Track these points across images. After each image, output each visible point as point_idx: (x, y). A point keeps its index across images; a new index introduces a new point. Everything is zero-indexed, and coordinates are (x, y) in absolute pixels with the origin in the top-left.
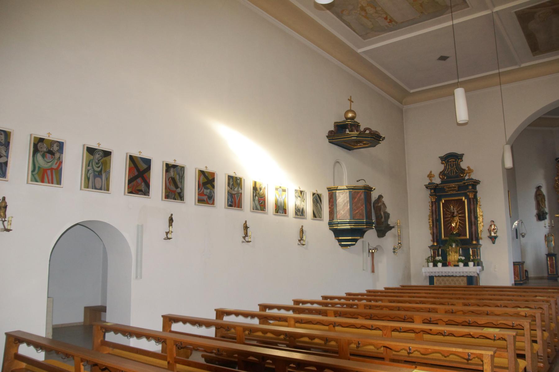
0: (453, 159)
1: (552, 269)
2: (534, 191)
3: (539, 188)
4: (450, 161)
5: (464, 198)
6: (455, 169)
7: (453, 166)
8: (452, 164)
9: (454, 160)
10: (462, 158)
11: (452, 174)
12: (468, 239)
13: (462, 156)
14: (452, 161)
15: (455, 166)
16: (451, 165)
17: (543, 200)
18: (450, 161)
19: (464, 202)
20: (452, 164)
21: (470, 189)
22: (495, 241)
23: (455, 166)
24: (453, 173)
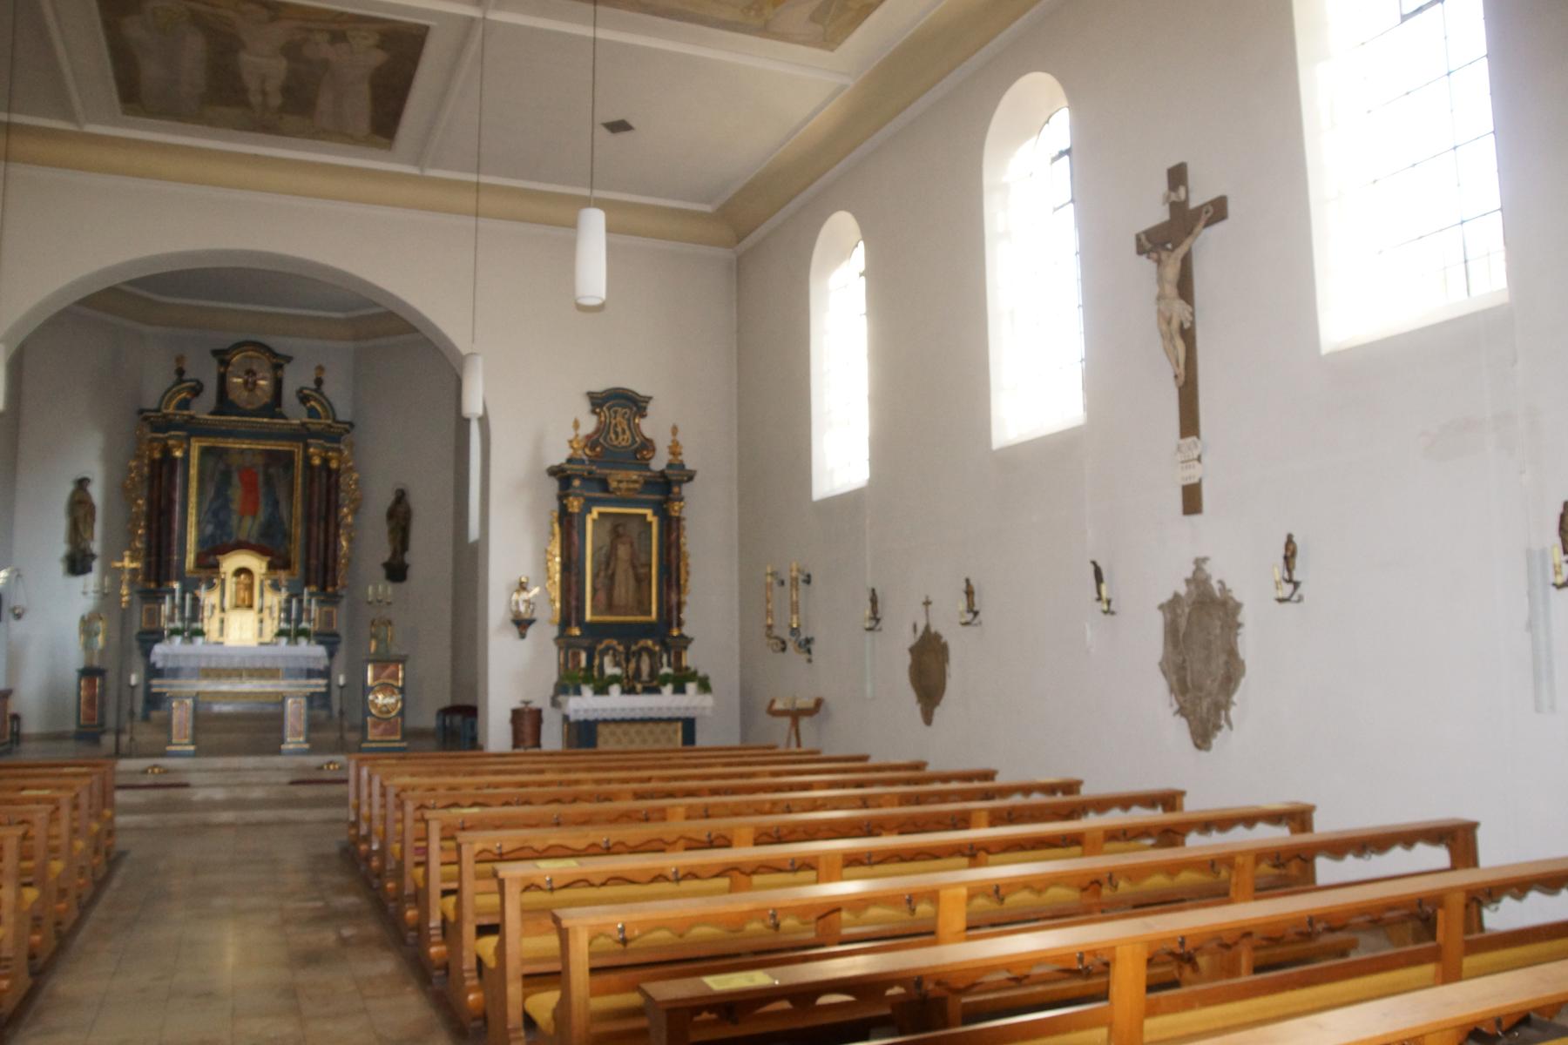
2: (68, 488)
3: (82, 484)
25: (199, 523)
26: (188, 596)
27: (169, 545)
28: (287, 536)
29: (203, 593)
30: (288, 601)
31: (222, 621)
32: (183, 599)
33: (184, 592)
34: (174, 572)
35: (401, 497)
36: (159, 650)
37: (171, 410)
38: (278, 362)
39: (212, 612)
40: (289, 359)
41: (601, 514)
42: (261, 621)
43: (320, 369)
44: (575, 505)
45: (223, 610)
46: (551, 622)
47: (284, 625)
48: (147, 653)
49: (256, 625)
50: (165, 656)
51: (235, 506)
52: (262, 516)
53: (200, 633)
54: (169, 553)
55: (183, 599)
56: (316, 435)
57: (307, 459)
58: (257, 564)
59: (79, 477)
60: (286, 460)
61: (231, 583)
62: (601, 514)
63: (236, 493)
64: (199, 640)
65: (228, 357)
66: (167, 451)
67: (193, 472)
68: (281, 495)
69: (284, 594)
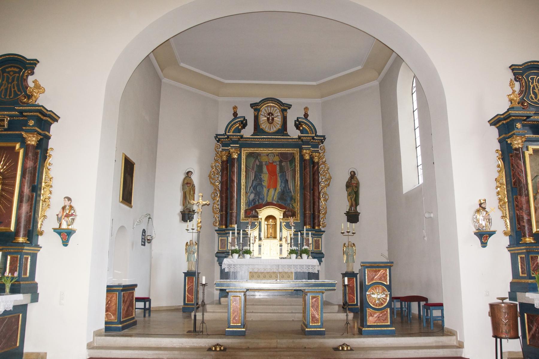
0: (14, 67)
1: (190, 296)
2: (183, 177)
3: (189, 173)
4: (9, 69)
5: (18, 146)
6: (14, 88)
7: (13, 81)
8: (11, 78)
9: (17, 70)
10: (34, 68)
11: (7, 97)
12: (12, 232)
13: (36, 64)
14: (13, 71)
15: (15, 82)
16: (8, 78)
17: (192, 192)
18: (7, 70)
19: (18, 153)
20: (11, 78)
21: (29, 126)
22: (68, 241)
23: (15, 82)
24: (10, 95)
25: (246, 193)
26: (241, 232)
27: (232, 204)
28: (292, 199)
29: (249, 231)
30: (296, 235)
31: (260, 246)
32: (239, 234)
33: (239, 230)
34: (234, 219)
35: (353, 175)
36: (226, 261)
37: (231, 134)
38: (285, 108)
39: (255, 241)
40: (289, 106)
41: (534, 150)
42: (281, 246)
43: (306, 109)
44: (517, 143)
45: (260, 239)
46: (505, 234)
47: (294, 248)
48: (220, 264)
49: (279, 248)
50: (229, 265)
51: (265, 184)
52: (279, 189)
53: (248, 252)
54: (232, 209)
55: (239, 234)
56: (307, 143)
57: (302, 156)
58: (277, 213)
59: (187, 171)
60: (291, 159)
61: (264, 224)
62: (534, 150)
63: (265, 177)
64: (247, 256)
65: (258, 107)
66: (229, 155)
67: (243, 167)
68: (289, 177)
69: (293, 230)
